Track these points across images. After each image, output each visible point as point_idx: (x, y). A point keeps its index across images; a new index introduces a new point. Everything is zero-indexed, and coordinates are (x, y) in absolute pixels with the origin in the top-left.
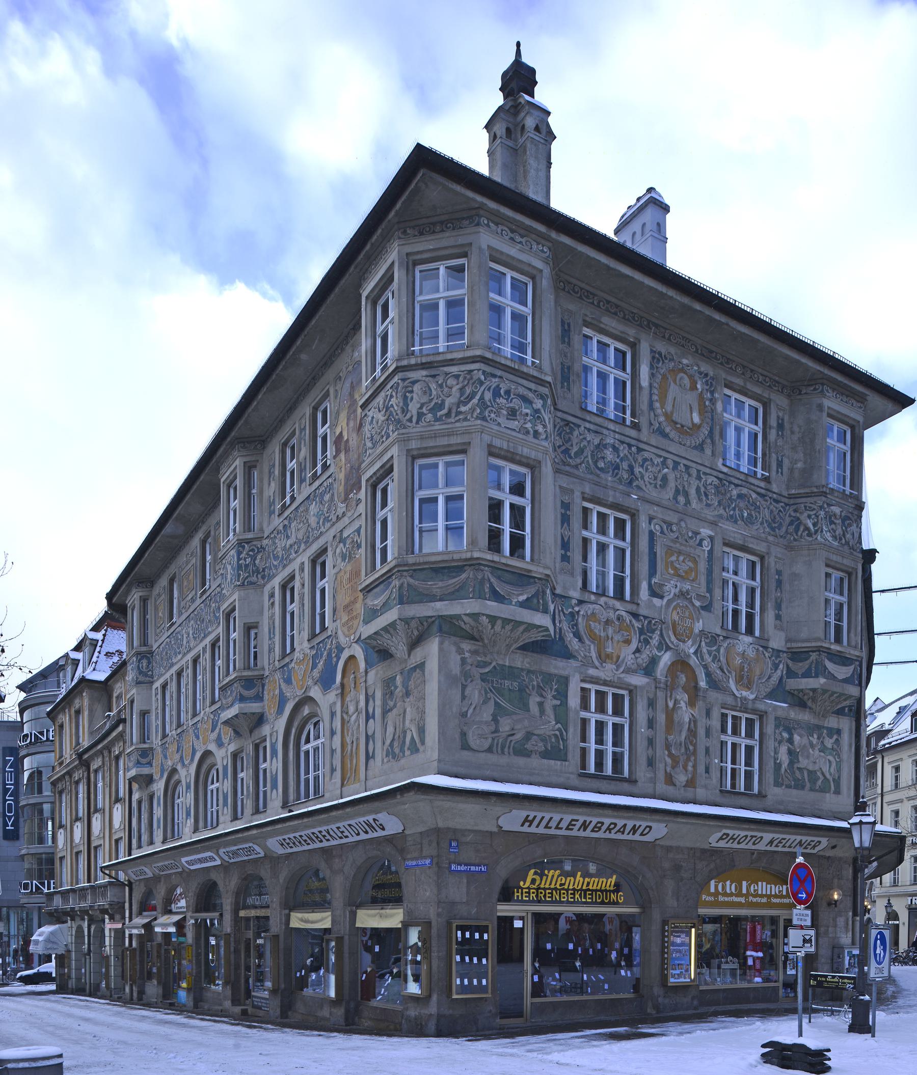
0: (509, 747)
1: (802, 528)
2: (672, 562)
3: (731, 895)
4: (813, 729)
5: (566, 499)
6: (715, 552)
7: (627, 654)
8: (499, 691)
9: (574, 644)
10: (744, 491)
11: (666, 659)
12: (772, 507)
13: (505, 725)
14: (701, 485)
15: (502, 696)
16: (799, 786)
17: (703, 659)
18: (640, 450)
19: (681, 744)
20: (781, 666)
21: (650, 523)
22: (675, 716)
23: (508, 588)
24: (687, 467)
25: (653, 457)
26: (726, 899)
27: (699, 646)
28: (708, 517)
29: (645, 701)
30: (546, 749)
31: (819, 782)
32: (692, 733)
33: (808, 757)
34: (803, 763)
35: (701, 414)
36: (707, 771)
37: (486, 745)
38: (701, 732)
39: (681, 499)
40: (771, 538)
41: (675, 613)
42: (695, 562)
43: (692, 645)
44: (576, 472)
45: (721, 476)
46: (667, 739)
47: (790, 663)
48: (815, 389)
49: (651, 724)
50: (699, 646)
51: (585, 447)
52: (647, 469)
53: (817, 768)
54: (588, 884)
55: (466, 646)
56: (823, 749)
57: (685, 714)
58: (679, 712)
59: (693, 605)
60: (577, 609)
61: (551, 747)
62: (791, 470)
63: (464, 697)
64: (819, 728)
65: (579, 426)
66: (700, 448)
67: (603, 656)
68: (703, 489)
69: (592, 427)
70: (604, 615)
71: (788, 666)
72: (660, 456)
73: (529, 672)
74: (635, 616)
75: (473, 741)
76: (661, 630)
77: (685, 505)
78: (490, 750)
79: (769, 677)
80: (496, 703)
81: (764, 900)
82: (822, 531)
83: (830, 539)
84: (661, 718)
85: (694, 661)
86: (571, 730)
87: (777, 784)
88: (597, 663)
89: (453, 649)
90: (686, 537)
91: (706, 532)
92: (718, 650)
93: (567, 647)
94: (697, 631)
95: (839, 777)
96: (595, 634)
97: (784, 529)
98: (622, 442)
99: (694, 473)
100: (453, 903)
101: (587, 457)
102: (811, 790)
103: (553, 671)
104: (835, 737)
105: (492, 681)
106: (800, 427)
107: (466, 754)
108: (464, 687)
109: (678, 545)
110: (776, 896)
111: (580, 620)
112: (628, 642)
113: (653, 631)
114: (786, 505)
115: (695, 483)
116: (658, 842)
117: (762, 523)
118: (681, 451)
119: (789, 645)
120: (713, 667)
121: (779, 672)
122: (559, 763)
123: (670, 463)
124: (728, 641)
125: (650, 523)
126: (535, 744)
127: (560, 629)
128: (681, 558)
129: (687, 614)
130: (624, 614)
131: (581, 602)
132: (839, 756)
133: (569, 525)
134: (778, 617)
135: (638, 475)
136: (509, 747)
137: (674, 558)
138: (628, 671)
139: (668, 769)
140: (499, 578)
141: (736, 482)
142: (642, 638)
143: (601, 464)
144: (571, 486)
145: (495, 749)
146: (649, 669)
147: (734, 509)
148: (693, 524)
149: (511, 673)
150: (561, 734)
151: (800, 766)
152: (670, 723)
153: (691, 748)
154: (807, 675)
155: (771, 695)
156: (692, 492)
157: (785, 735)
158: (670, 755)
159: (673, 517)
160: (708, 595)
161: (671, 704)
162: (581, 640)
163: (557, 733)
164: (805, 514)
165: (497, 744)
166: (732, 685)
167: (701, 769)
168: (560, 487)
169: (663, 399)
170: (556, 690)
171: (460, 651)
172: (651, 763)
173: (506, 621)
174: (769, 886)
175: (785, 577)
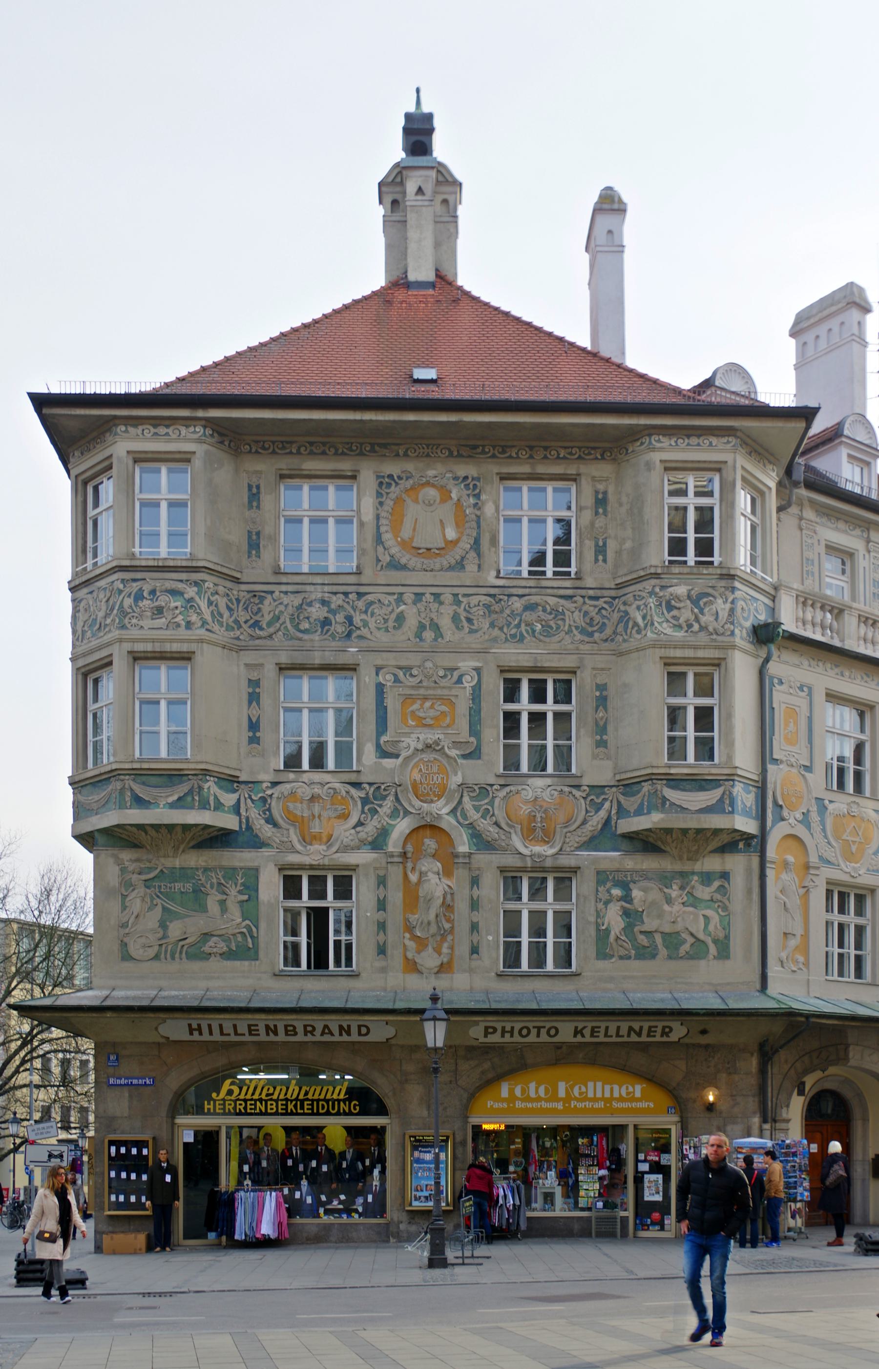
0: (181, 953)
1: (630, 624)
2: (413, 712)
3: (539, 1099)
4: (665, 879)
5: (254, 676)
6: (484, 687)
7: (344, 832)
8: (168, 896)
9: (266, 831)
10: (534, 599)
11: (402, 827)
12: (585, 608)
13: (175, 930)
14: (461, 611)
15: (173, 900)
16: (646, 953)
17: (465, 817)
18: (360, 595)
19: (429, 923)
20: (607, 805)
21: (377, 674)
22: (420, 890)
23: (155, 791)
24: (436, 596)
25: (382, 597)
26: (530, 1105)
27: (460, 802)
28: (473, 646)
29: (373, 880)
30: (230, 949)
31: (686, 947)
32: (448, 907)
33: (660, 916)
34: (650, 923)
35: (459, 524)
36: (475, 950)
37: (152, 952)
38: (462, 906)
39: (428, 635)
40: (585, 648)
41: (416, 771)
42: (452, 704)
43: (446, 804)
44: (268, 642)
45: (493, 591)
46: (407, 920)
47: (622, 798)
48: (642, 444)
49: (382, 905)
50: (460, 802)
51: (281, 612)
52: (372, 615)
53: (679, 927)
54: (306, 1093)
55: (126, 855)
56: (694, 902)
57: (435, 884)
58: (426, 886)
59: (448, 756)
60: (269, 792)
61: (237, 946)
62: (619, 553)
63: (124, 908)
64: (683, 875)
65: (272, 593)
66: (460, 565)
67: (308, 839)
68: (463, 615)
69: (290, 588)
70: (305, 792)
71: (619, 803)
72: (394, 594)
73: (206, 870)
74: (357, 785)
75: (135, 950)
76: (396, 795)
77: (435, 640)
78: (157, 957)
79: (584, 822)
80: (164, 908)
81: (601, 1104)
82: (652, 624)
83: (669, 631)
84: (395, 897)
85: (448, 822)
86: (263, 925)
87: (602, 955)
88: (299, 847)
89: (111, 861)
90: (435, 678)
91: (467, 664)
92: (491, 803)
93: (257, 836)
94: (453, 786)
95: (727, 937)
96: (295, 816)
97: (608, 631)
98: (335, 593)
99: (447, 598)
100: (113, 1118)
101: (284, 622)
102: (670, 957)
103: (237, 864)
104: (716, 884)
105: (160, 887)
106: (628, 495)
107: (127, 965)
108: (124, 897)
109: (422, 691)
110: (621, 1099)
111: (274, 804)
112: (345, 816)
113: (384, 798)
114: (614, 598)
115: (448, 610)
116: (393, 1042)
117: (569, 632)
118: (428, 578)
119: (618, 777)
120: (484, 825)
121: (603, 814)
122: (246, 963)
123: (409, 597)
124: (508, 789)
125: (377, 674)
126: (215, 945)
127: (247, 819)
128: (428, 704)
129: (435, 769)
130: (337, 786)
131: (275, 784)
132: (725, 908)
133: (258, 704)
134: (601, 743)
135: (360, 624)
136: (181, 953)
137: (416, 706)
138: (346, 849)
139: (410, 955)
140: (144, 784)
141: (520, 591)
142: (366, 808)
143: (305, 625)
144: (261, 661)
145: (163, 956)
146: (377, 843)
147: (518, 626)
148: (447, 661)
149: (184, 874)
150: (250, 931)
151: (645, 928)
153: (447, 926)
154: (639, 812)
155: (591, 843)
156: (445, 623)
157: (617, 892)
158: (414, 938)
159: (411, 660)
160: (472, 739)
161: (413, 878)
162: (275, 825)
163: (244, 930)
164: (634, 606)
165: (166, 951)
166: (517, 842)
167: (463, 949)
168: (246, 665)
169: (396, 526)
170: (243, 884)
171: (119, 862)
172: (382, 950)
173: (156, 827)
174: (607, 1088)
175: (611, 692)
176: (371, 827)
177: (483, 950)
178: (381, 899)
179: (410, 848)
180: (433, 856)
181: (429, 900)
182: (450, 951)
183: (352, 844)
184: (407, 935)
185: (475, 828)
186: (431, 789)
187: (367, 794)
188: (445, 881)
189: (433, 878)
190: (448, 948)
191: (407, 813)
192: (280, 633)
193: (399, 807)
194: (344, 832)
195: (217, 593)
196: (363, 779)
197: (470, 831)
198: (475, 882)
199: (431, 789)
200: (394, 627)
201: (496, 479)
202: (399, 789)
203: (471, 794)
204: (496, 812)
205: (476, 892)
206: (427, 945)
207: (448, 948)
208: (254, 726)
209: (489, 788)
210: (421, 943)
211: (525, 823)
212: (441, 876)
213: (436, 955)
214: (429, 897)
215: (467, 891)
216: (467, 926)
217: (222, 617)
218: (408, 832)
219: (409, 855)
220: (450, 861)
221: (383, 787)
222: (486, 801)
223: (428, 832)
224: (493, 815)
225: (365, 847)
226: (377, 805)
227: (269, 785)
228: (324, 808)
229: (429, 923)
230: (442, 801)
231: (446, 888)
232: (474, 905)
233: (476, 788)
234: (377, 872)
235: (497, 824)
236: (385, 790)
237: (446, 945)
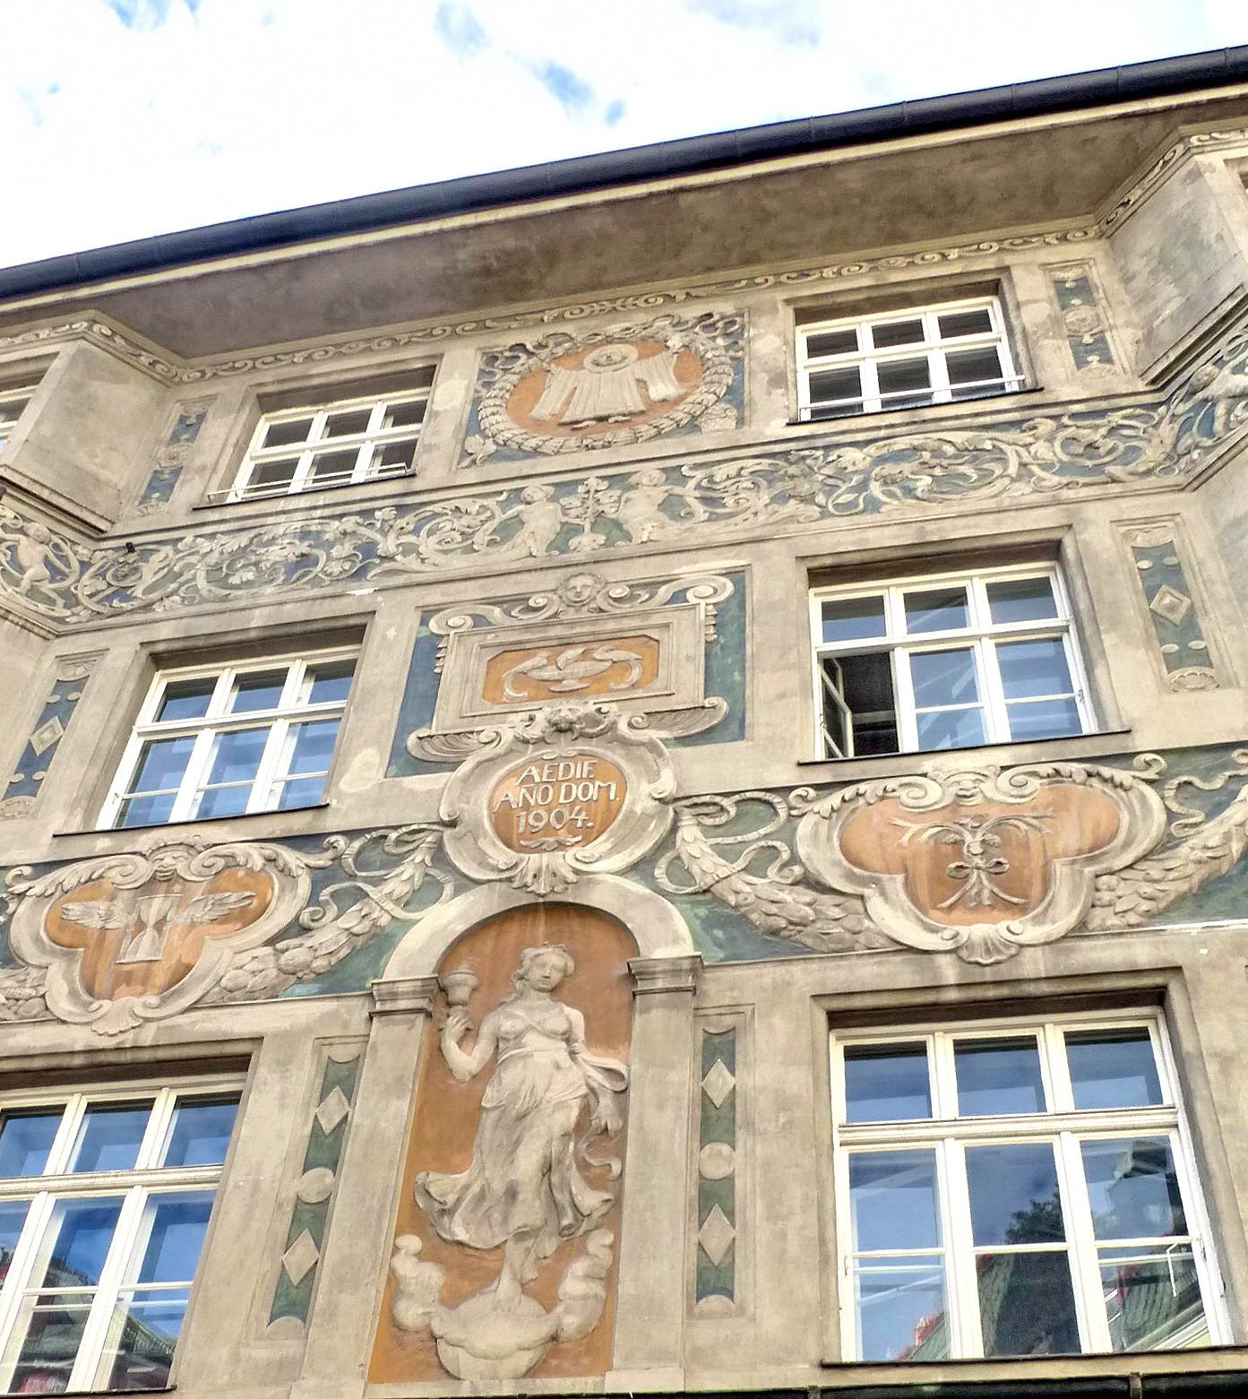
19: (512, 1193)
29: (305, 1074)
32: (599, 1137)
36: (713, 1279)
49: (324, 1149)
58: (510, 1077)
67: (103, 983)
84: (383, 1113)
90: (600, 602)
96: (82, 931)
139: (410, 1314)
152: (450, 1116)
153: (590, 1200)
158: (441, 1250)
161: (465, 1060)
166: (892, 917)
172: (293, 1300)
176: (331, 936)
177: (753, 1280)
178: (327, 1126)
179: (462, 980)
180: (554, 991)
181: (522, 1117)
182: (598, 1289)
183: (251, 982)
184: (412, 1243)
185: (723, 902)
186: (559, 817)
187: (337, 858)
189: (543, 1052)
190: (588, 1277)
191: (466, 883)
192: (175, 598)
194: (233, 956)
195: (22, 531)
196: (329, 822)
197: (702, 912)
198: (719, 1047)
199: (559, 817)
200: (491, 543)
201: (788, 314)
202: (448, 833)
203: (708, 821)
204: (802, 851)
205: (720, 1081)
206: (498, 1273)
207: (588, 1277)
208: (33, 761)
209: (775, 799)
210: (468, 1269)
211: (923, 866)
212: (578, 1047)
213: (531, 1306)
214: (520, 1106)
215: (682, 1076)
216: (675, 1193)
217: (22, 570)
218: (461, 928)
219: (460, 994)
220: (618, 988)
221: (393, 835)
222: (762, 832)
223: (541, 927)
224: (794, 859)
225: (299, 989)
226: (366, 880)
227: (27, 871)
228: (181, 904)
229: (512, 1193)
230: (601, 844)
231: (599, 1078)
232: (715, 1122)
233: (725, 802)
234: (326, 1051)
235: (812, 882)
236: (399, 842)
237: (579, 1267)
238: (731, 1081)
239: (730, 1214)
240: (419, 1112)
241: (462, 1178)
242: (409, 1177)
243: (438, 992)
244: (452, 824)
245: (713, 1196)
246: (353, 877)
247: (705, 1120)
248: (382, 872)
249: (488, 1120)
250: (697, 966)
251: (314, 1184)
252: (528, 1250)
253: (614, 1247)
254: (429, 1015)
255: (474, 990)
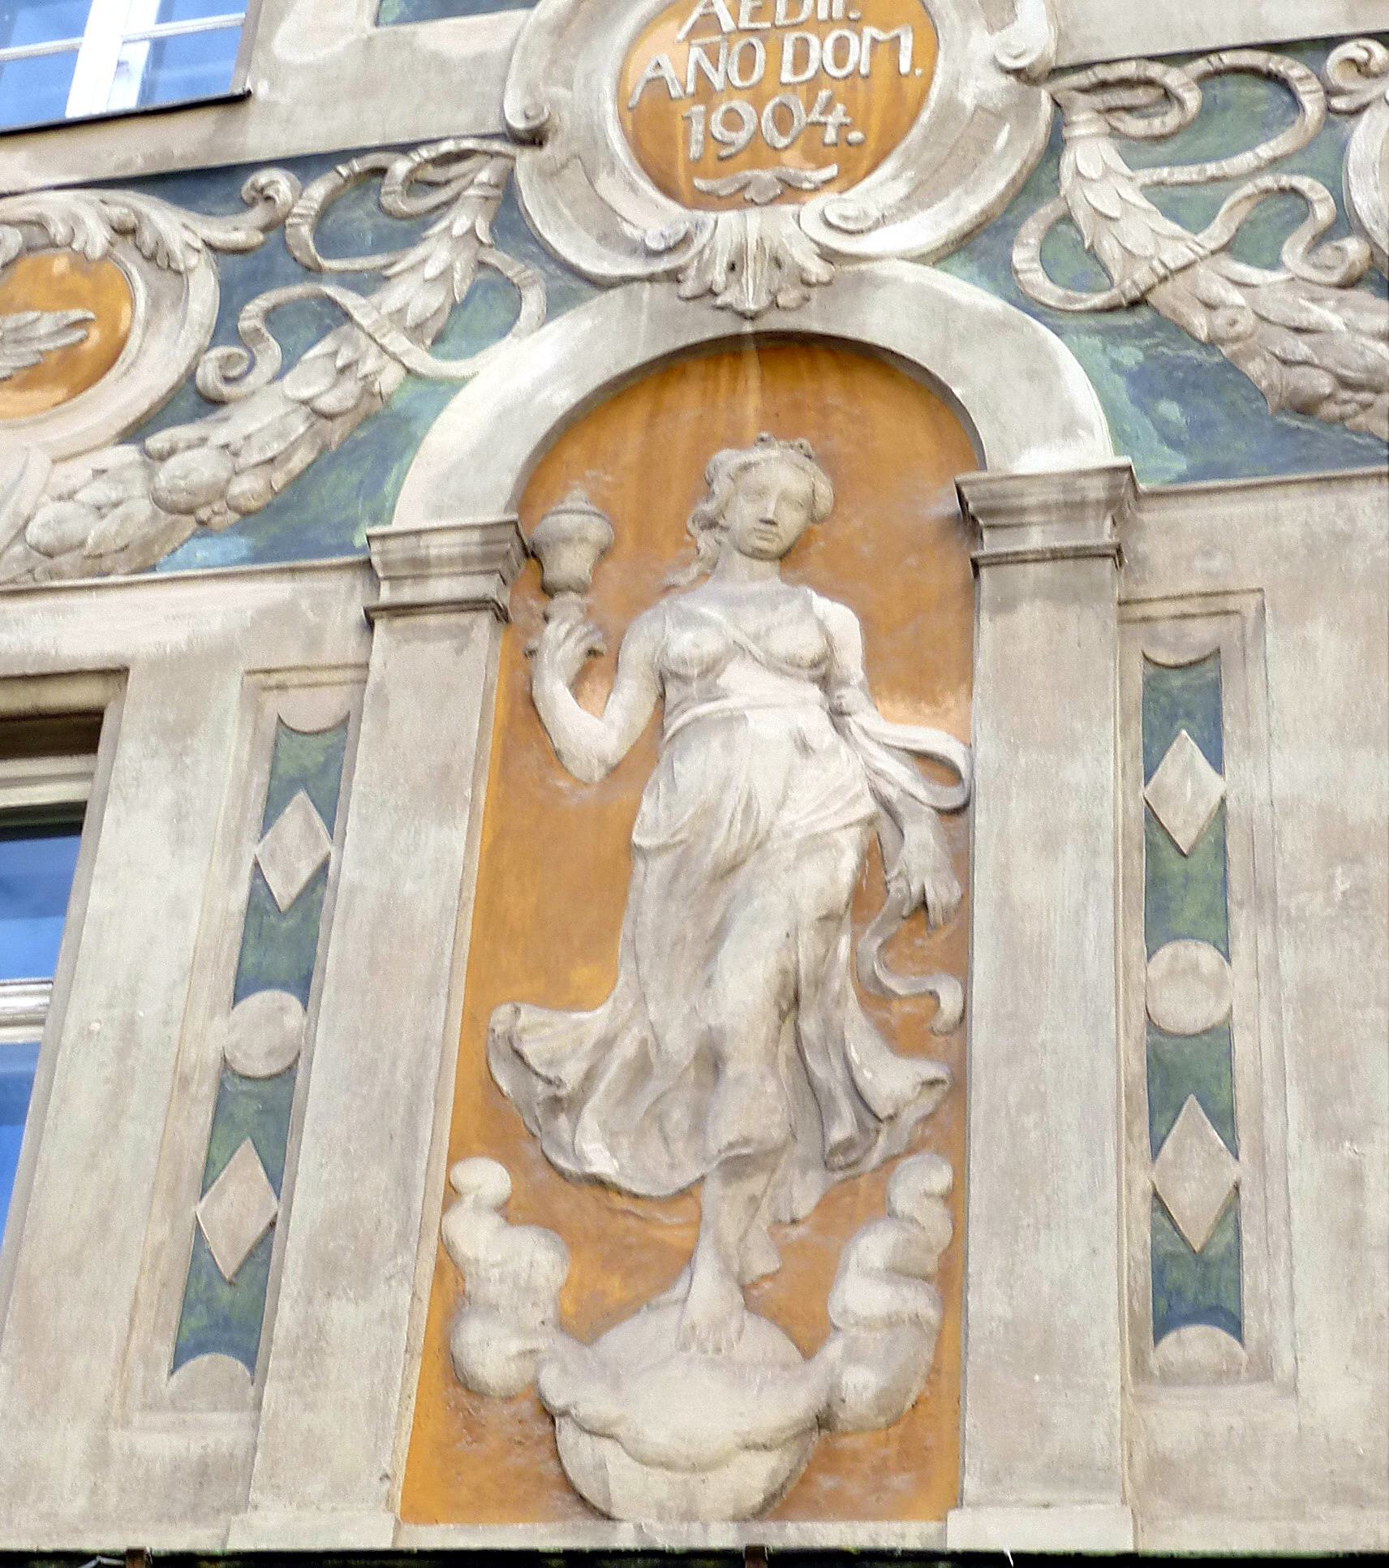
19: (711, 1060)
29: (228, 758)
32: (907, 921)
36: (1191, 1287)
38: (1050, 891)
43: (917, 199)
49: (279, 945)
58: (695, 769)
84: (409, 862)
139: (492, 1352)
152: (561, 869)
153: (893, 1079)
158: (553, 1195)
161: (591, 729)
176: (272, 416)
178: (284, 891)
179: (575, 529)
180: (787, 558)
181: (727, 871)
182: (919, 1302)
183: (95, 531)
184: (487, 1178)
185: (1180, 331)
186: (783, 118)
188: (889, 728)
189: (769, 711)
190: (898, 1272)
191: (573, 286)
193: (514, 269)
196: (255, 137)
197: (1130, 355)
198: (1184, 702)
199: (783, 118)
202: (525, 160)
203: (1135, 126)
204: (1363, 200)
205: (1189, 785)
206: (688, 1258)
207: (898, 1272)
209: (1292, 68)
210: (620, 1248)
212: (851, 697)
213: (762, 1341)
214: (722, 843)
215: (1096, 767)
216: (1099, 1067)
218: (564, 397)
219: (570, 563)
220: (941, 556)
221: (401, 167)
222: (1265, 151)
223: (751, 393)
224: (1345, 222)
225: (204, 551)
229: (711, 1060)
230: (883, 187)
231: (902, 776)
232: (1180, 887)
233: (1173, 78)
234: (274, 704)
236: (416, 184)
237: (874, 1247)
238: (1215, 786)
239: (1224, 1120)
240: (491, 855)
241: (596, 1021)
242: (475, 1020)
243: (519, 555)
244: (535, 139)
245: (1182, 1077)
246: (313, 272)
247: (1156, 882)
248: (379, 260)
249: (650, 877)
250: (1122, 493)
251: (260, 1029)
252: (754, 1201)
253: (955, 1199)
254: (502, 616)
255: (604, 553)
